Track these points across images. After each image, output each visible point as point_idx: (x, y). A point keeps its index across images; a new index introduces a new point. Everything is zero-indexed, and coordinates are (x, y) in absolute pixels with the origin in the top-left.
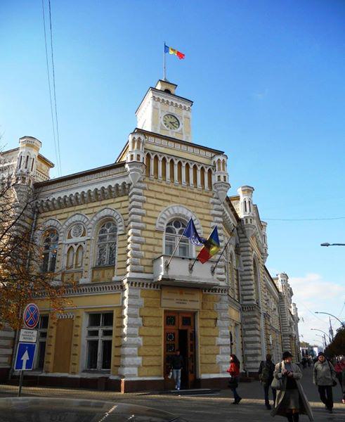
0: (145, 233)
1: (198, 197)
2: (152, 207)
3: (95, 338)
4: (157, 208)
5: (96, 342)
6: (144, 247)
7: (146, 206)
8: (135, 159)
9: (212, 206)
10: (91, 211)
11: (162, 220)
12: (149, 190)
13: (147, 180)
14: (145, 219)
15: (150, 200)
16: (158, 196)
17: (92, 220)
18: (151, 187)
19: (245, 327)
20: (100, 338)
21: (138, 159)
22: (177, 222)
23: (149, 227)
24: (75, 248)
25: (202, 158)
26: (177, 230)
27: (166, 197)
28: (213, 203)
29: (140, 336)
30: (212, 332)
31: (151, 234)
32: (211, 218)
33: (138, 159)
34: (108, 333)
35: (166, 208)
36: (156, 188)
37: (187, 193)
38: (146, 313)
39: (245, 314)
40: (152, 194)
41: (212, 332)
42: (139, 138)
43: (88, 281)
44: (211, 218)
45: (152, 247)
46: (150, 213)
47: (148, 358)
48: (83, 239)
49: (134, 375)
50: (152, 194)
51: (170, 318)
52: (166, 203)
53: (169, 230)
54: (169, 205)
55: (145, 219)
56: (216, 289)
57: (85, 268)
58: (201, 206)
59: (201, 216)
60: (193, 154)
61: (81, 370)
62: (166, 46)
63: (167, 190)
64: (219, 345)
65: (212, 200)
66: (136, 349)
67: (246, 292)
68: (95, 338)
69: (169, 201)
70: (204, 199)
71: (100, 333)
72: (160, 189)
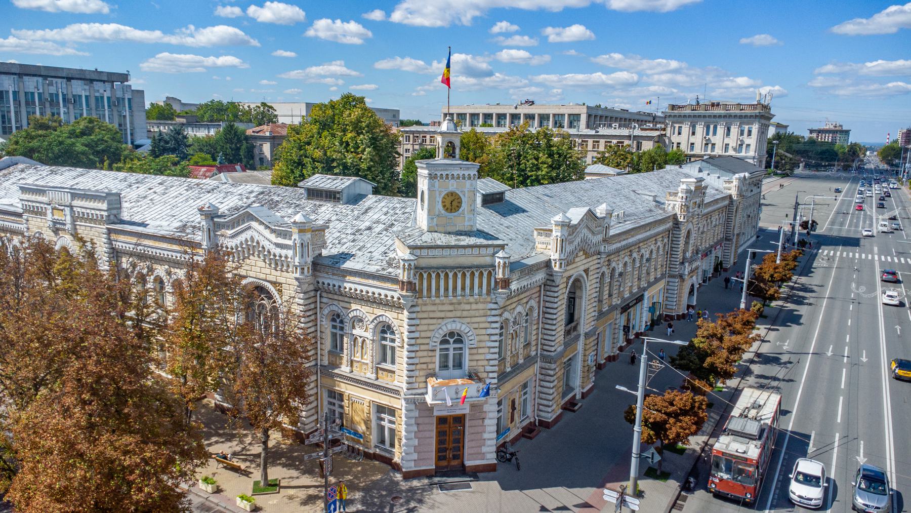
0: (420, 354)
1: (474, 306)
2: (425, 328)
4: (431, 327)
6: (419, 367)
7: (419, 328)
9: (489, 313)
11: (435, 340)
13: (420, 301)
14: (419, 341)
15: (424, 322)
16: (432, 315)
17: (373, 321)
18: (424, 308)
20: (386, 424)
22: (452, 334)
23: (423, 347)
26: (452, 341)
27: (442, 315)
30: (480, 429)
31: (425, 354)
32: (487, 325)
35: (439, 326)
38: (420, 421)
40: (425, 315)
41: (480, 429)
44: (487, 325)
45: (425, 365)
46: (423, 335)
49: (410, 468)
50: (425, 315)
52: (440, 320)
53: (445, 341)
55: (419, 341)
58: (477, 315)
59: (476, 326)
61: (373, 445)
62: (448, 85)
63: (441, 308)
64: (485, 439)
67: (546, 342)
70: (481, 306)
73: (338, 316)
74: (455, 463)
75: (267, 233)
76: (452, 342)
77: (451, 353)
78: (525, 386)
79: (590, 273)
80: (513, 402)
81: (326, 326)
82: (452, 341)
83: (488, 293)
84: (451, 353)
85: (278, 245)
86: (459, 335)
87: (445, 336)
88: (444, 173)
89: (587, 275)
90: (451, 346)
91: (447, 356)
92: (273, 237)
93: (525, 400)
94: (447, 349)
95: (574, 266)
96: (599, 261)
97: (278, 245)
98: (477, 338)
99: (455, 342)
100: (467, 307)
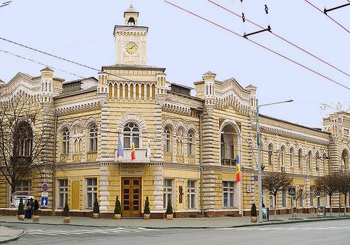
1: (145, 106)
2: (114, 118)
3: (90, 192)
10: (84, 118)
13: (110, 101)
19: (204, 181)
21: (102, 91)
22: (131, 125)
24: (78, 140)
25: (148, 77)
26: (132, 129)
30: (152, 188)
32: (154, 119)
33: (102, 91)
34: (96, 189)
36: (116, 105)
39: (203, 172)
43: (85, 161)
44: (154, 119)
48: (80, 135)
51: (126, 181)
57: (83, 153)
60: (143, 75)
65: (154, 106)
68: (90, 192)
70: (149, 106)
71: (93, 189)
72: (116, 105)
73: (67, 130)
74: (135, 212)
75: (27, 84)
78: (191, 183)
79: (242, 127)
81: (60, 137)
82: (132, 129)
83: (153, 98)
85: (33, 89)
86: (136, 125)
87: (127, 125)
88: (127, 32)
89: (240, 126)
90: (132, 133)
92: (31, 86)
93: (193, 196)
95: (225, 113)
97: (33, 89)
98: (147, 127)
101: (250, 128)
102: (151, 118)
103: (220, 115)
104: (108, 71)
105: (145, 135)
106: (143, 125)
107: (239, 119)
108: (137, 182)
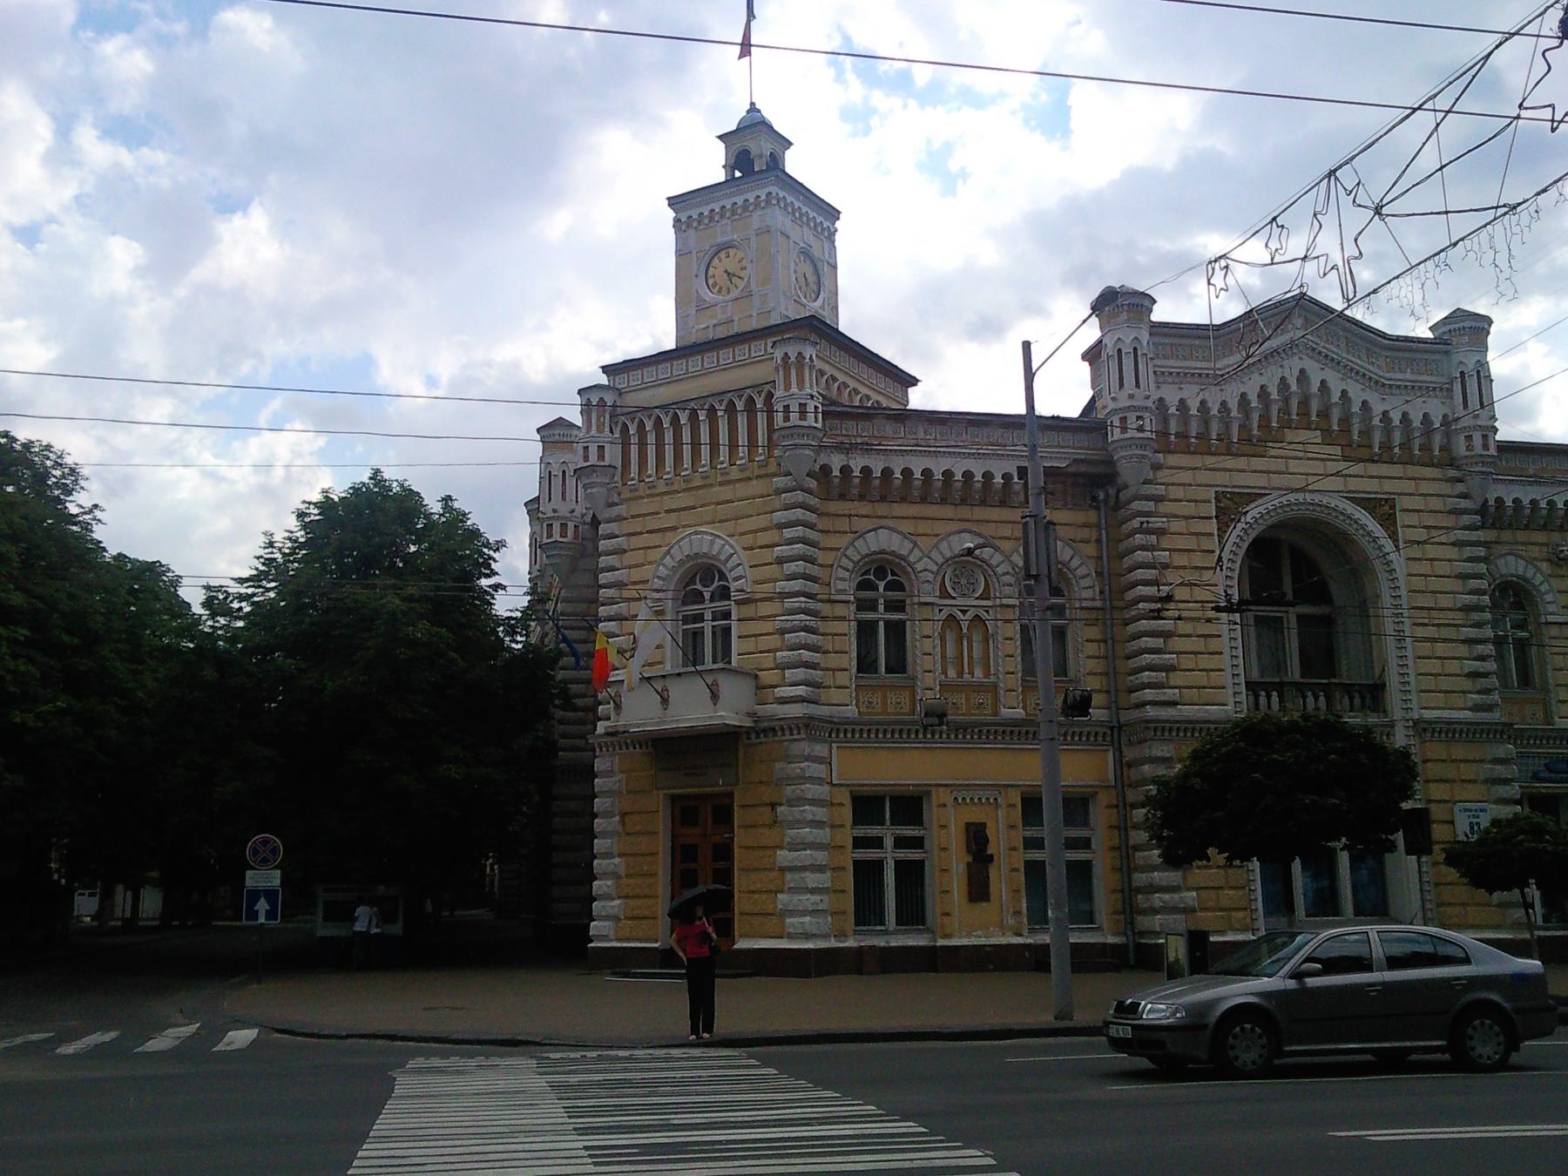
1: (742, 490)
5: (878, 865)
7: (629, 559)
8: (593, 460)
9: (776, 502)
11: (658, 583)
12: (633, 517)
16: (653, 524)
21: (601, 457)
28: (779, 492)
29: (620, 855)
33: (601, 457)
36: (646, 506)
37: (717, 488)
40: (636, 526)
42: (601, 399)
47: (632, 903)
50: (636, 526)
54: (672, 538)
56: (773, 730)
64: (782, 870)
66: (609, 883)
69: (674, 528)
70: (756, 487)
76: (707, 596)
77: (708, 626)
80: (977, 838)
82: (707, 596)
84: (708, 626)
89: (1388, 521)
90: (708, 608)
91: (697, 635)
94: (699, 618)
96: (1460, 488)
99: (712, 600)
100: (725, 492)
101: (1466, 519)
102: (764, 538)
103: (1220, 478)
104: (621, 382)
105: (748, 611)
106: (742, 578)
107: (1372, 485)
108: (724, 814)
